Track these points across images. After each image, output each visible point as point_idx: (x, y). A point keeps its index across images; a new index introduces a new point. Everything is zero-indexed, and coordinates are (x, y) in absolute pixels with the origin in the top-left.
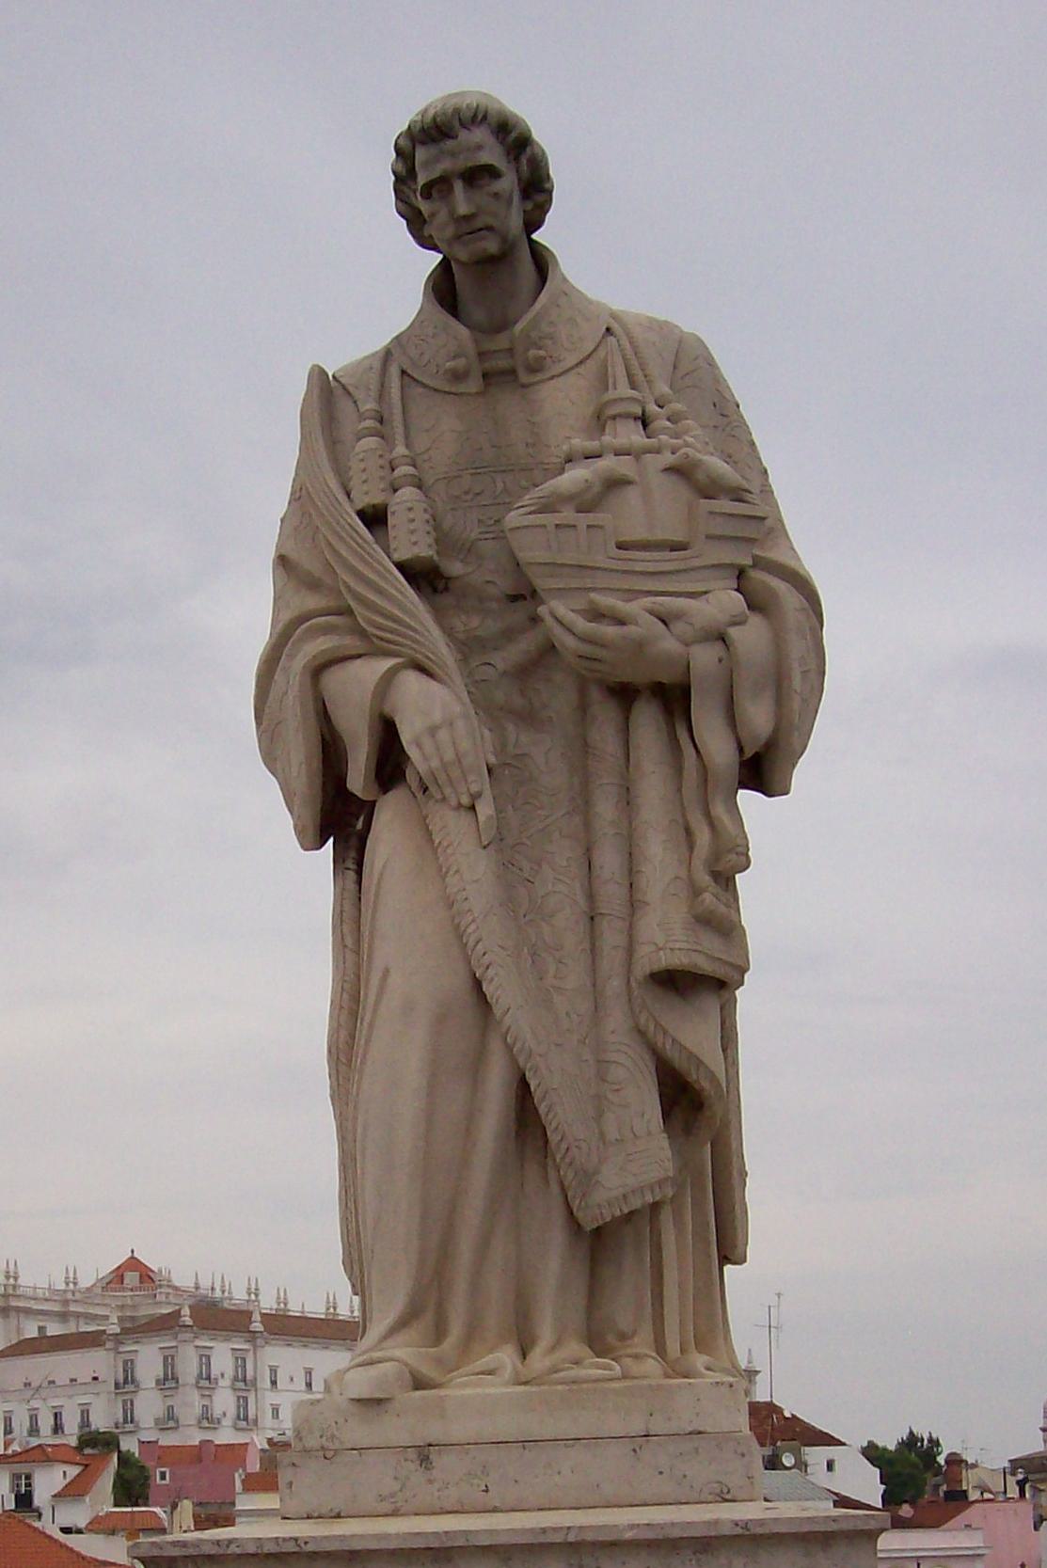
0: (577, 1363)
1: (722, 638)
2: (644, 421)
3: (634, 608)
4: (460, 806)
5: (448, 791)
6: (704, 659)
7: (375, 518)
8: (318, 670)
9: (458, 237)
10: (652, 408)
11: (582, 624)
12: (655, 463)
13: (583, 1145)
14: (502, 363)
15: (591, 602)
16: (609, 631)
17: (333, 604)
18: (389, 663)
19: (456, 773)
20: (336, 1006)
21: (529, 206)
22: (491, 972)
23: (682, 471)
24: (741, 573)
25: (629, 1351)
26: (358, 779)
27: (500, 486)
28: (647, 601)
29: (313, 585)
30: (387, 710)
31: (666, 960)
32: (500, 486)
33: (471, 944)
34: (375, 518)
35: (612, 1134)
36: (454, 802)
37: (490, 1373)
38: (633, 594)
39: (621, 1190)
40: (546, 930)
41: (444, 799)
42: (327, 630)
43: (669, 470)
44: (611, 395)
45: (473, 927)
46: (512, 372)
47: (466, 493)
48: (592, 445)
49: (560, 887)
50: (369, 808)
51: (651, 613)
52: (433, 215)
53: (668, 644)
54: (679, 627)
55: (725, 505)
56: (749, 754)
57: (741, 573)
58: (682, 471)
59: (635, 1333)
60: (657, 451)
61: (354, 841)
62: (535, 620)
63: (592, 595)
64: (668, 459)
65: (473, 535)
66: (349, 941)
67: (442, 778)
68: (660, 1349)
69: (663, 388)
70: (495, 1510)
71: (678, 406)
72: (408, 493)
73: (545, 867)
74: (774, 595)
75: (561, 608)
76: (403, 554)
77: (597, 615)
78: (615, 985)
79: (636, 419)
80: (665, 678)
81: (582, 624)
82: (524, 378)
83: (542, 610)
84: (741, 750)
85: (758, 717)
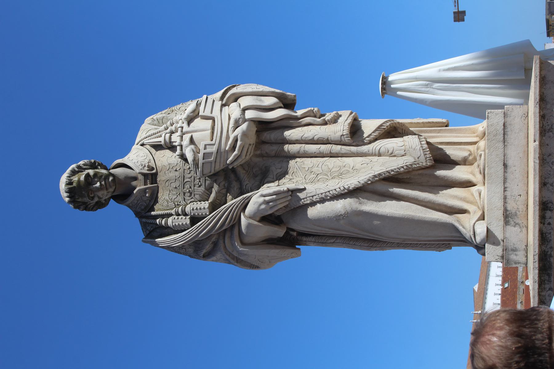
0: (478, 166)
1: (244, 110)
2: (172, 133)
4: (291, 195)
6: (249, 114)
7: (194, 220)
8: (243, 244)
9: (107, 189)
10: (168, 131)
12: (186, 128)
13: (405, 162)
16: (239, 143)
17: (221, 238)
20: (354, 246)
21: (99, 167)
22: (346, 187)
23: (190, 120)
24: (223, 105)
25: (476, 151)
26: (280, 232)
28: (230, 132)
29: (215, 244)
31: (346, 132)
34: (194, 220)
35: (403, 153)
36: (290, 198)
37: (480, 194)
38: (228, 137)
39: (422, 151)
40: (334, 170)
43: (189, 124)
45: (331, 192)
46: (152, 174)
48: (178, 148)
49: (320, 166)
50: (289, 230)
52: (99, 197)
55: (202, 108)
56: (282, 106)
57: (223, 105)
58: (190, 120)
59: (469, 151)
60: (182, 128)
61: (299, 238)
62: (233, 170)
64: (185, 125)
66: (332, 241)
68: (475, 143)
69: (162, 128)
70: (527, 193)
71: (169, 123)
72: (188, 209)
73: (313, 170)
74: (233, 94)
77: (233, 148)
78: (353, 149)
79: (171, 135)
80: (255, 129)
81: (236, 152)
82: (154, 171)
83: (230, 167)
84: (280, 107)
85: (270, 101)
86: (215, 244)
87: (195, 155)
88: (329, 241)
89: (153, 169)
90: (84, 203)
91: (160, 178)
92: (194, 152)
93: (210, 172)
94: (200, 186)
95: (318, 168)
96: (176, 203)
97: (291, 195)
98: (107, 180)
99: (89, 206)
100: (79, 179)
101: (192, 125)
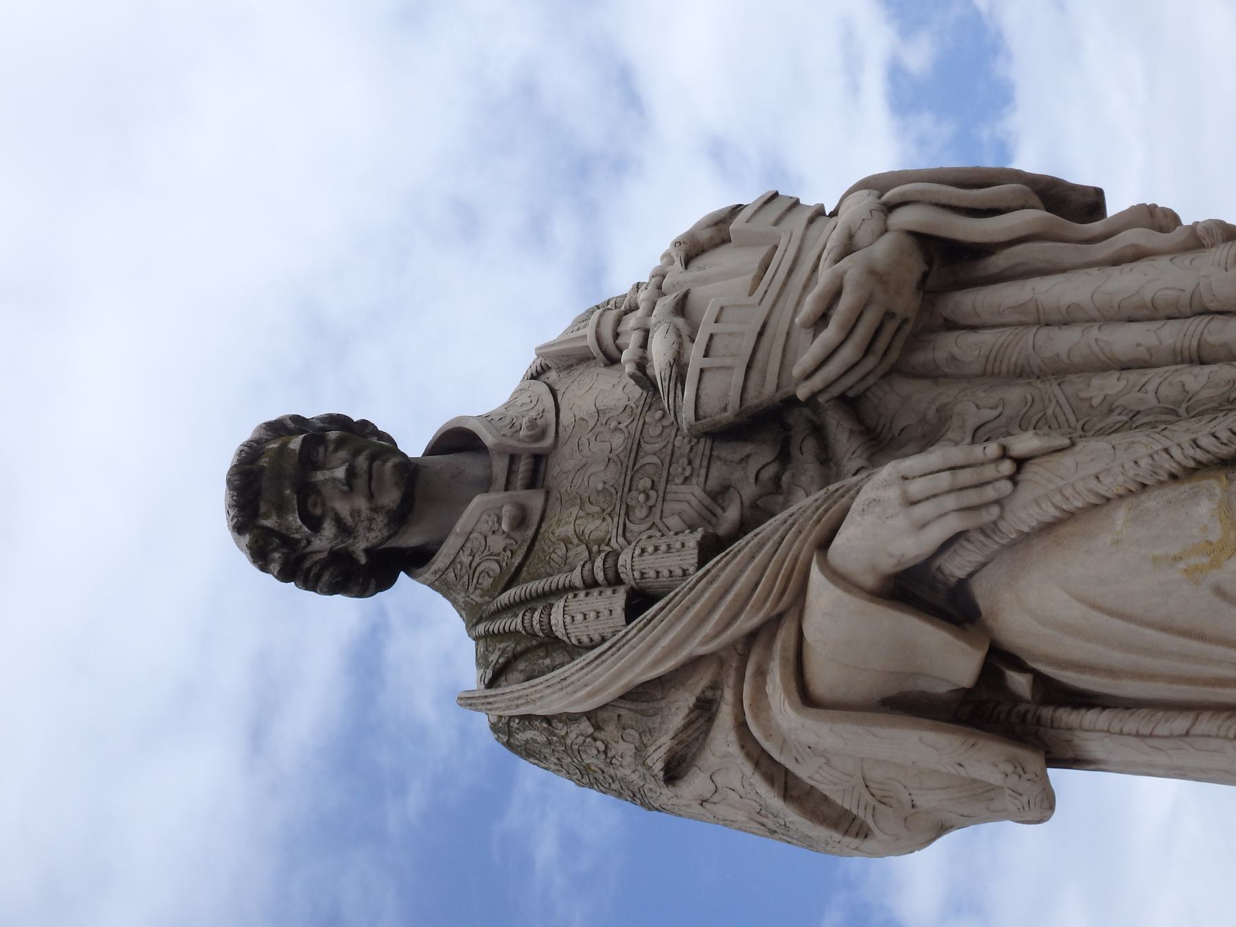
3: (825, 275)
5: (990, 493)
8: (806, 698)
11: (830, 334)
14: (523, 467)
15: (805, 325)
16: (846, 302)
18: (816, 574)
19: (965, 477)
27: (655, 460)
30: (869, 581)
32: (655, 460)
33: (1199, 454)
36: (1006, 486)
40: (1205, 394)
41: (998, 502)
42: (761, 673)
44: (595, 350)
45: (1176, 452)
47: (648, 498)
51: (836, 262)
53: (881, 250)
54: (862, 236)
63: (797, 320)
65: (698, 491)
67: (972, 497)
75: (806, 358)
76: (690, 557)
77: (821, 320)
81: (830, 334)
83: (802, 393)
86: (705, 708)
87: (681, 345)
88: (1162, 729)
89: (542, 435)
90: (287, 541)
91: (563, 466)
92: (680, 336)
93: (725, 409)
94: (686, 480)
95: (1141, 395)
96: (595, 548)
97: (1013, 479)
98: (377, 464)
99: (307, 564)
100: (283, 448)
101: (696, 264)
